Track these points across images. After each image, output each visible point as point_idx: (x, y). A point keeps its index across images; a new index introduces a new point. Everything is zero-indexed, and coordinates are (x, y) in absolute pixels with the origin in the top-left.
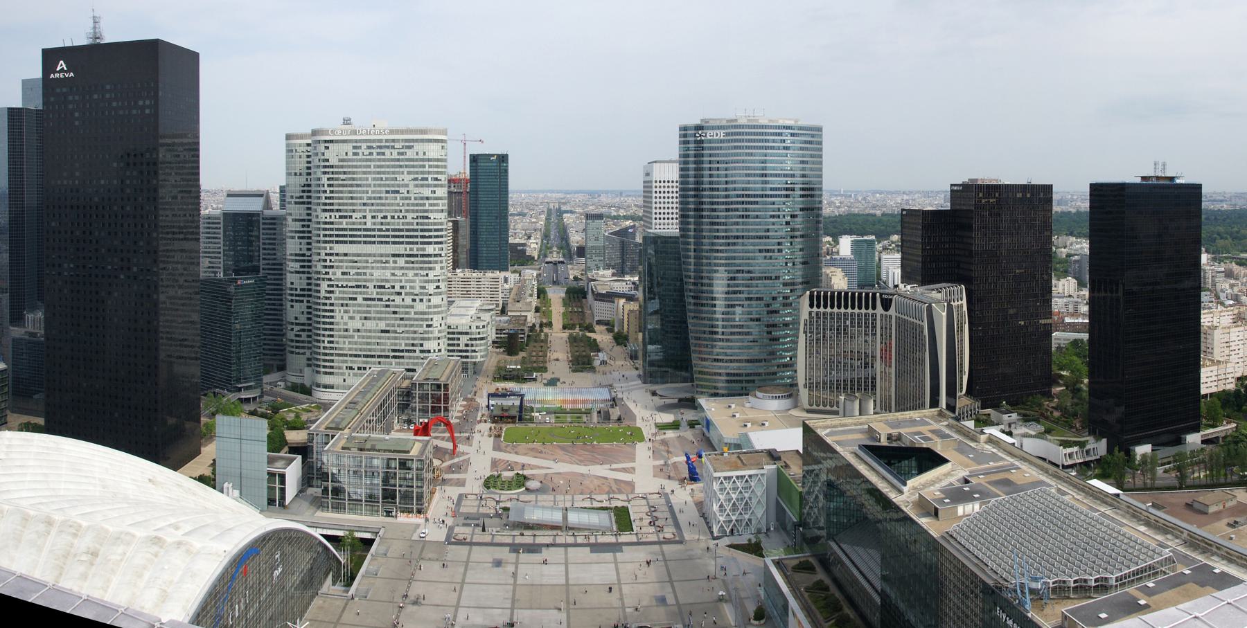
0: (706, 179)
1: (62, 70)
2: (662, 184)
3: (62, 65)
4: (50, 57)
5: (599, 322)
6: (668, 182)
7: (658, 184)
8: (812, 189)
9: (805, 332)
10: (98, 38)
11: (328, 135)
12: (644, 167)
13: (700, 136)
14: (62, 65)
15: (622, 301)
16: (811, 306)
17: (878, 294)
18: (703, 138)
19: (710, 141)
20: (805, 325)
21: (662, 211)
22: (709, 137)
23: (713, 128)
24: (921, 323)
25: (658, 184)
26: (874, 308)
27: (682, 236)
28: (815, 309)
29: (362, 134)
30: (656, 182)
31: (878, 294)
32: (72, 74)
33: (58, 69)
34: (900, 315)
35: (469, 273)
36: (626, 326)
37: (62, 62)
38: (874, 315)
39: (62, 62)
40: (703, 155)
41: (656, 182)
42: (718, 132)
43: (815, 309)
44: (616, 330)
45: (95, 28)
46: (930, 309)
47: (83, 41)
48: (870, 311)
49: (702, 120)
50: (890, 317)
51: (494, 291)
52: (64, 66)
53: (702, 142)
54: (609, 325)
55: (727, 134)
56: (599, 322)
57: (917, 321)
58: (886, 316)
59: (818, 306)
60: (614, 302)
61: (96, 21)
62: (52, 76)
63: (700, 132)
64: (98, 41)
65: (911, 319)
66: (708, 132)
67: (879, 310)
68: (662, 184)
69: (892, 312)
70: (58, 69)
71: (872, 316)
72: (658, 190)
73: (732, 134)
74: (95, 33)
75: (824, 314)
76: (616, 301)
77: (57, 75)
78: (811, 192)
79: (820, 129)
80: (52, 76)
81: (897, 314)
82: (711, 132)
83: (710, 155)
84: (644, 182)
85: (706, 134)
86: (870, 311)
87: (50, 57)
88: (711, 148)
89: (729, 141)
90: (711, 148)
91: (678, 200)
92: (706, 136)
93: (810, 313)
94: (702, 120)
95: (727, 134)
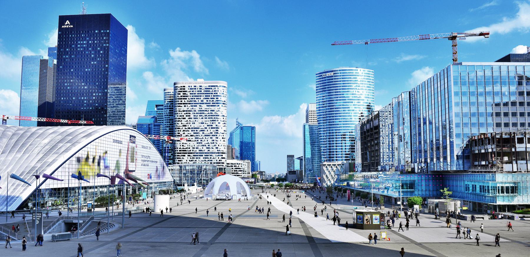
1: (68, 24)
2: (312, 112)
3: (68, 22)
7: (311, 112)
14: (68, 22)
25: (311, 112)
30: (310, 111)
32: (72, 26)
33: (66, 23)
37: (68, 21)
39: (68, 21)
41: (310, 111)
52: (69, 23)
62: (63, 27)
70: (66, 23)
77: (65, 26)
80: (63, 27)
82: (328, 73)
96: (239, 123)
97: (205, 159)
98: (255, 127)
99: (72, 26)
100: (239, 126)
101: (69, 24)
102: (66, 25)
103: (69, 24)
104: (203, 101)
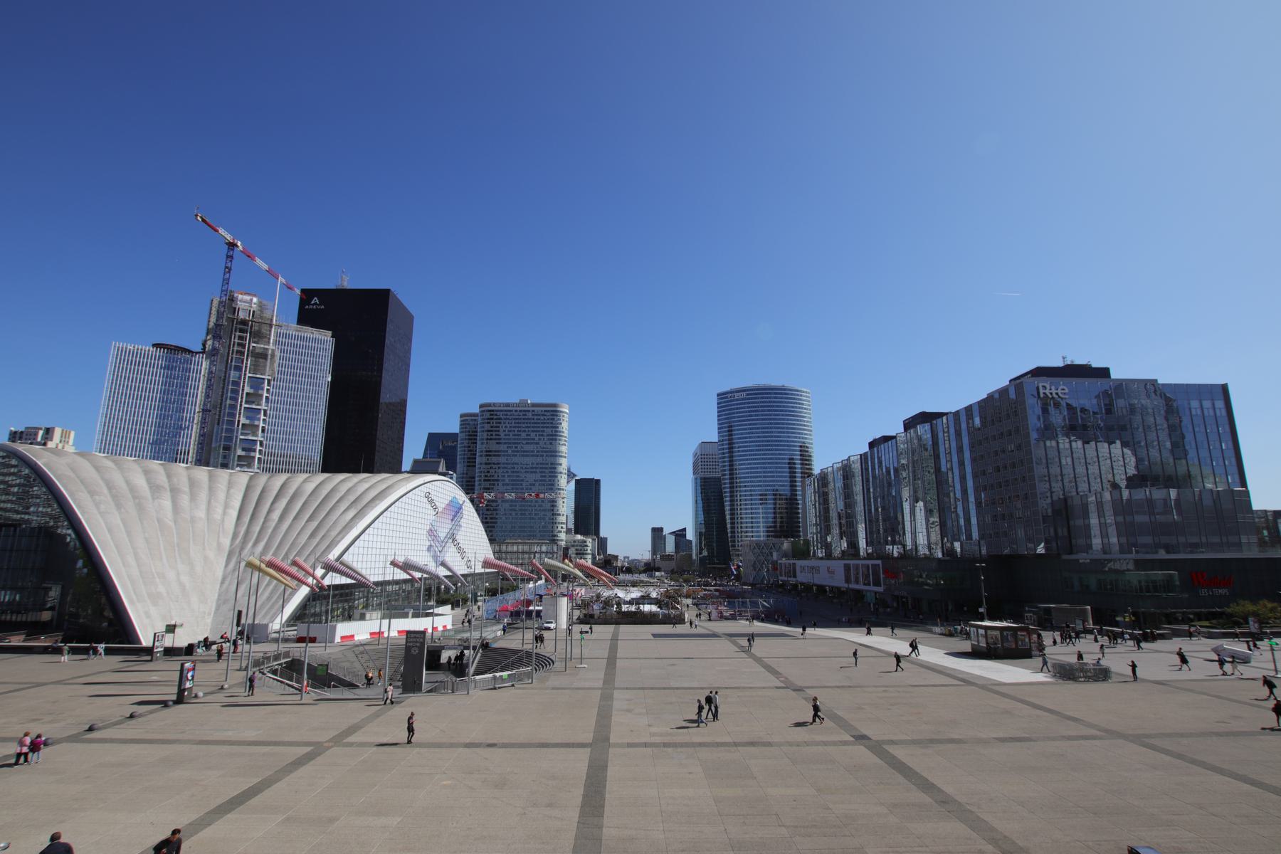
1: (315, 304)
3: (316, 300)
14: (316, 300)
21: (709, 467)
32: (323, 307)
33: (313, 302)
52: (317, 301)
55: (748, 395)
62: (307, 307)
70: (313, 302)
72: (703, 460)
73: (751, 394)
77: (311, 307)
80: (307, 307)
95: (748, 395)
99: (323, 307)
102: (313, 305)
104: (529, 435)
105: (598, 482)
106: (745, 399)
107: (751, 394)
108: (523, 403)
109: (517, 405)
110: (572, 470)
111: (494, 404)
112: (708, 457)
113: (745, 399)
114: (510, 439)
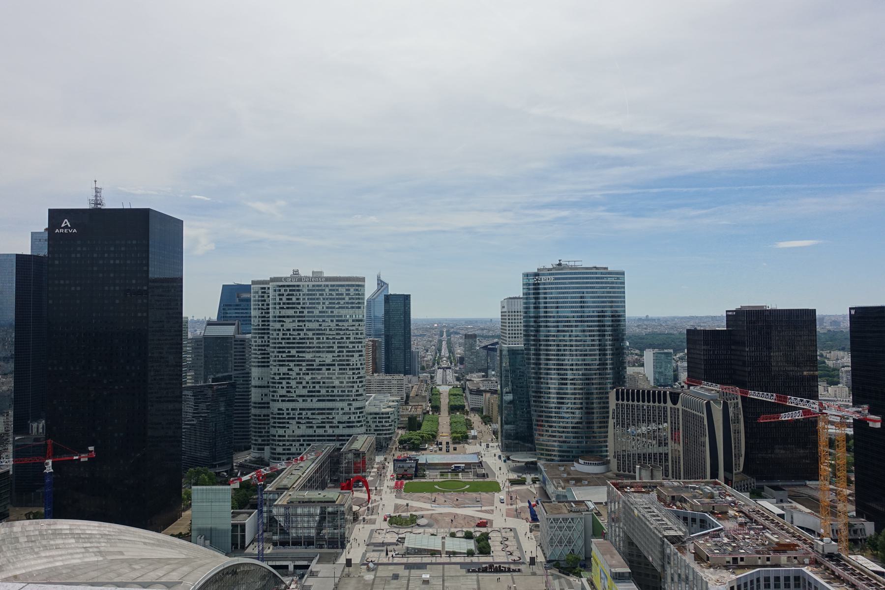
0: (542, 310)
1: (66, 227)
3: (66, 222)
4: (56, 216)
5: (473, 409)
6: (518, 312)
8: (619, 316)
9: (613, 418)
10: (100, 204)
11: (282, 281)
12: (502, 302)
13: (537, 280)
14: (66, 222)
15: (488, 395)
16: (618, 399)
17: (668, 392)
18: (539, 282)
19: (544, 284)
20: (613, 413)
21: (514, 332)
22: (543, 281)
23: (544, 275)
24: (701, 415)
25: (510, 314)
26: (665, 402)
27: (526, 349)
28: (620, 402)
29: (306, 281)
30: (509, 312)
31: (668, 392)
32: (75, 231)
33: (63, 225)
34: (685, 409)
35: (382, 376)
36: (491, 412)
38: (665, 409)
39: (66, 220)
40: (539, 294)
42: (549, 277)
43: (620, 402)
44: (484, 414)
45: (96, 196)
46: (708, 404)
47: (86, 206)
48: (662, 404)
49: (538, 269)
50: (678, 410)
51: (400, 388)
53: (539, 284)
54: (478, 410)
55: (556, 279)
56: (473, 409)
57: (699, 414)
58: (675, 409)
59: (623, 400)
60: (482, 395)
61: (97, 191)
62: (57, 231)
63: (537, 278)
64: (99, 206)
65: (690, 410)
66: (543, 277)
67: (669, 404)
68: (513, 314)
69: (679, 405)
70: (63, 225)
71: (664, 408)
73: (559, 279)
74: (96, 200)
75: (622, 405)
76: (484, 395)
77: (62, 231)
78: (617, 319)
79: (623, 274)
80: (57, 231)
81: (683, 408)
83: (545, 293)
84: (502, 312)
85: (541, 279)
86: (662, 404)
87: (56, 216)
88: (545, 289)
89: (557, 283)
90: (545, 289)
91: (522, 325)
92: (541, 280)
93: (617, 405)
94: (538, 269)
95: (556, 279)
96: (381, 281)
97: (328, 416)
98: (410, 295)
99: (75, 231)
100: (382, 287)
101: (69, 226)
102: (64, 228)
103: (69, 226)
105: (406, 298)
106: (552, 284)
107: (559, 279)
108: (317, 276)
109: (309, 279)
110: (382, 278)
111: (286, 279)
112: (516, 314)
113: (552, 284)
114: (304, 317)
